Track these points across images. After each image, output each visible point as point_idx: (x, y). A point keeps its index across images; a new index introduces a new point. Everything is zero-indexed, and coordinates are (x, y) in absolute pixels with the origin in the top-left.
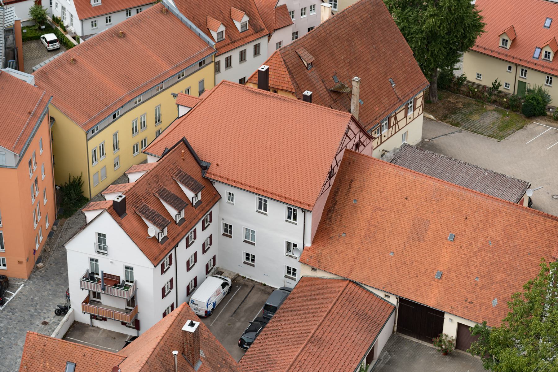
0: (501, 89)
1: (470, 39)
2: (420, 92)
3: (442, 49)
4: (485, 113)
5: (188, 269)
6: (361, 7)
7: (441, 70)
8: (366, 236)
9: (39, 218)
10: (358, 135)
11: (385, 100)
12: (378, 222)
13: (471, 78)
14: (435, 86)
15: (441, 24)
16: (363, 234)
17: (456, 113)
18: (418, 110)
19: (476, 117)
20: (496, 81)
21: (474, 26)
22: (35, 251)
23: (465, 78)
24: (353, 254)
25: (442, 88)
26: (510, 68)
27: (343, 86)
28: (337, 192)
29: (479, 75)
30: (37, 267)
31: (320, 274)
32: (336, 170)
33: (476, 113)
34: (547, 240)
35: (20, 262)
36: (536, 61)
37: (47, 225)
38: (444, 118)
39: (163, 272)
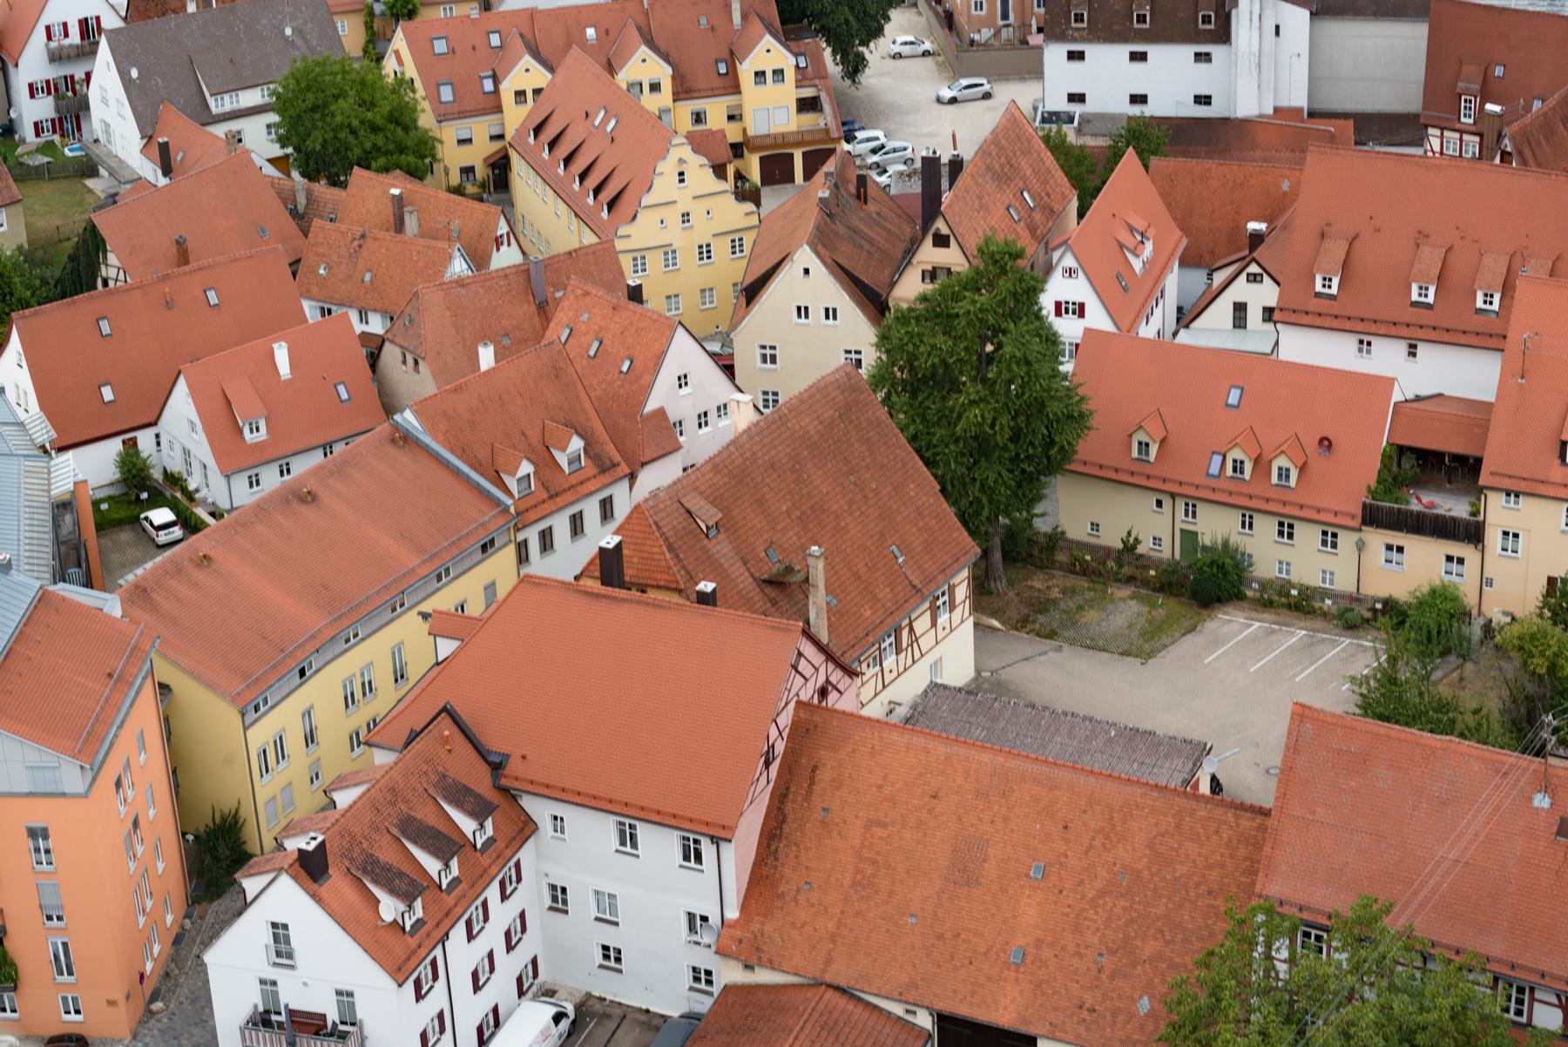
0: (1140, 550)
1: (1062, 448)
2: (961, 569)
3: (1005, 473)
4: (1111, 607)
5: (477, 988)
6: (818, 396)
7: (1007, 521)
8: (854, 884)
9: (149, 904)
10: (822, 670)
11: (884, 593)
12: (878, 853)
13: (1077, 530)
14: (997, 556)
15: (995, 419)
16: (847, 882)
17: (1047, 610)
18: (958, 611)
19: (1091, 615)
20: (1129, 534)
21: (1070, 416)
22: (142, 976)
23: (1063, 533)
24: (831, 926)
25: (1015, 560)
26: (1159, 504)
27: (789, 570)
28: (785, 796)
29: (1095, 526)
30: (150, 1012)
31: (764, 976)
32: (780, 747)
33: (1091, 607)
34: (1245, 859)
35: (112, 1003)
36: (1214, 483)
37: (169, 919)
38: (1022, 624)
39: (419, 997)
